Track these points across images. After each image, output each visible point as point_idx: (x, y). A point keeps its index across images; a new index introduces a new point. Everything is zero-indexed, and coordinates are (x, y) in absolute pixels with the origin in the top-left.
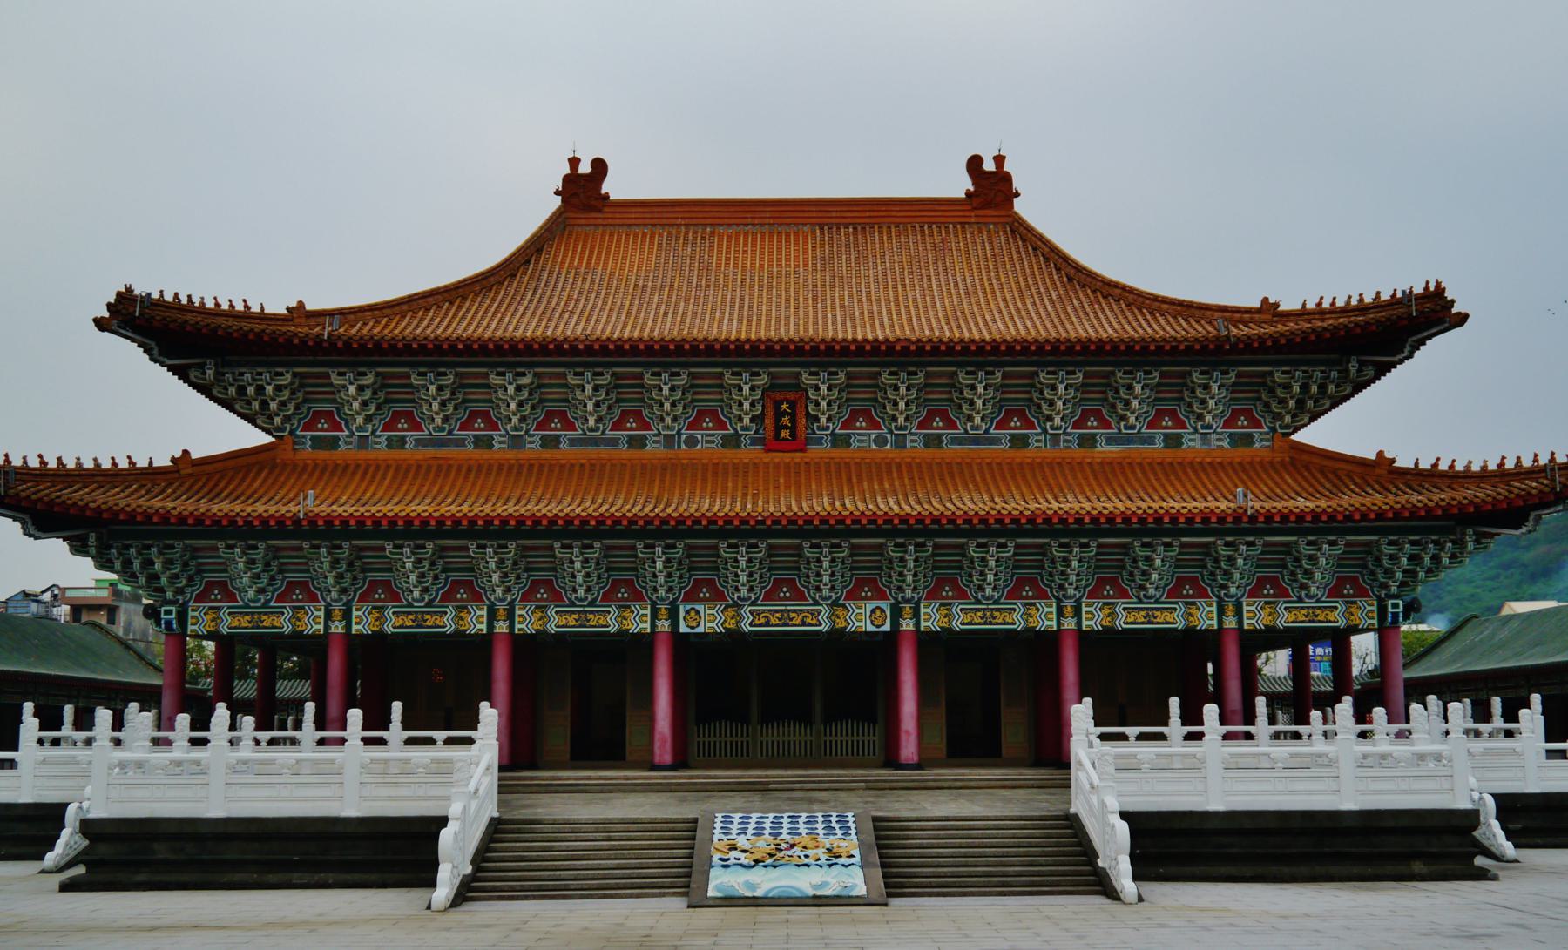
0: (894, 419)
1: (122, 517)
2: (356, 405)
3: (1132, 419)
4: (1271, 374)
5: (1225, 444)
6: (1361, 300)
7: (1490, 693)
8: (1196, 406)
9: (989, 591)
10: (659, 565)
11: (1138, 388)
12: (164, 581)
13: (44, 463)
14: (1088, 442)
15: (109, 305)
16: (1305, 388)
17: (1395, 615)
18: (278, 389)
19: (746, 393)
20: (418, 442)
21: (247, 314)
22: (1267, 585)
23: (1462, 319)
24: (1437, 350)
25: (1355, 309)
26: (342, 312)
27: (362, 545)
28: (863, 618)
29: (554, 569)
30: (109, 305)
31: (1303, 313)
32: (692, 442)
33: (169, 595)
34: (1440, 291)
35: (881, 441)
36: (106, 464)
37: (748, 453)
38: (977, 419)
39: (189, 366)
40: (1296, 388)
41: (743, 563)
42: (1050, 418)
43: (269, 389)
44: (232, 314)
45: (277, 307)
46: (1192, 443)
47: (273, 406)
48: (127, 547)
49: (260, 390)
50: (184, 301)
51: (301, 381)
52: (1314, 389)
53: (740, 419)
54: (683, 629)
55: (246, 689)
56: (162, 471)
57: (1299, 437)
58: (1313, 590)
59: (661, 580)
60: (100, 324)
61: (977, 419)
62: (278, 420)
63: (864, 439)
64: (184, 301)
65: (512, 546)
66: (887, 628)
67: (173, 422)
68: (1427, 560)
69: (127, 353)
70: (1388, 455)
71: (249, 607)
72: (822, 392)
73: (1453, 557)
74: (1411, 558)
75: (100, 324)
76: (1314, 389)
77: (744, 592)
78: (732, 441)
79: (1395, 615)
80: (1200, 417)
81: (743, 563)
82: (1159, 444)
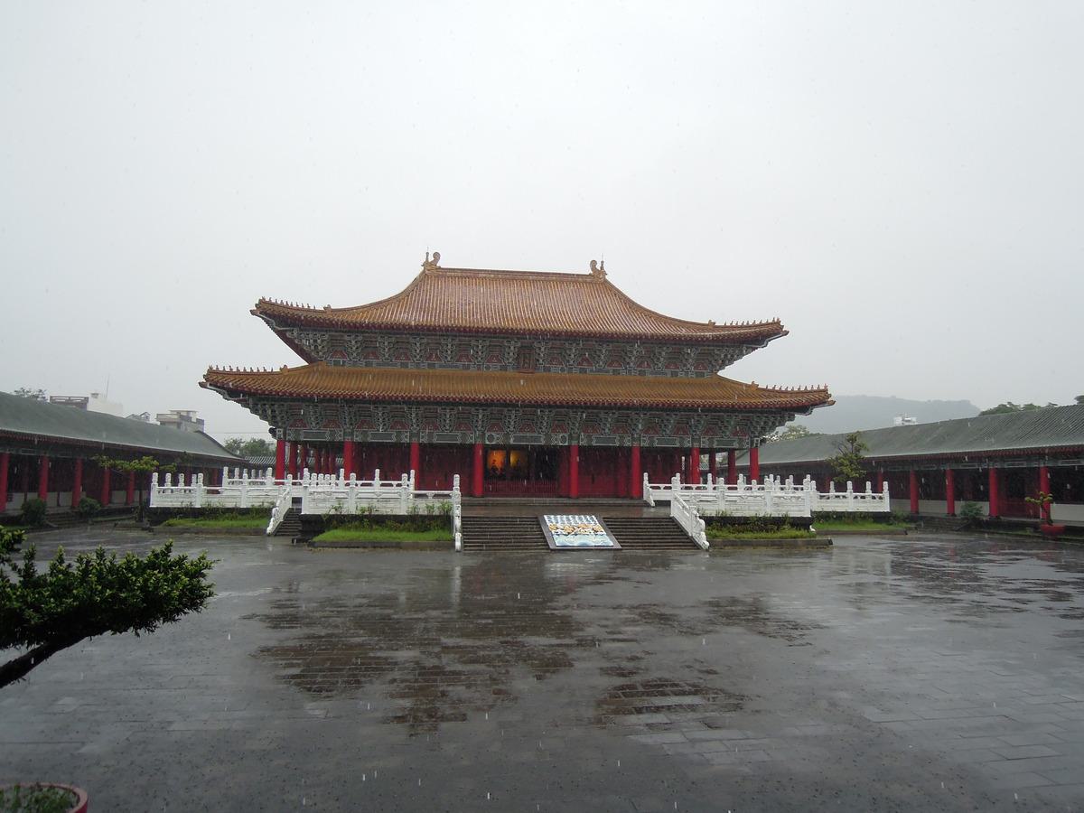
0: (568, 361)
1: (267, 392)
2: (354, 348)
3: (660, 365)
4: (713, 350)
5: (694, 376)
6: (748, 323)
7: (792, 472)
8: (684, 361)
9: (607, 430)
10: (480, 417)
11: (664, 353)
12: (279, 418)
13: (231, 369)
14: (642, 373)
15: (256, 305)
16: (726, 356)
17: (757, 444)
18: (322, 341)
19: (513, 347)
20: (378, 364)
21: (309, 310)
22: (708, 431)
23: (786, 333)
24: (774, 344)
25: (746, 327)
26: (344, 310)
27: (359, 406)
28: (558, 440)
29: (436, 418)
30: (256, 305)
31: (725, 327)
32: (488, 368)
33: (280, 424)
34: (778, 322)
35: (562, 370)
36: (255, 371)
37: (510, 373)
38: (601, 363)
39: (286, 331)
40: (722, 356)
41: (513, 417)
42: (628, 363)
43: (319, 341)
44: (303, 309)
45: (320, 307)
46: (681, 375)
47: (320, 348)
48: (265, 405)
49: (315, 341)
50: (285, 304)
51: (332, 339)
52: (729, 356)
53: (508, 359)
54: (488, 443)
55: (311, 461)
56: (277, 373)
57: (721, 373)
58: (728, 433)
59: (480, 423)
60: (253, 312)
61: (601, 363)
62: (320, 353)
63: (556, 370)
64: (285, 304)
65: (422, 408)
66: (566, 444)
67: (273, 355)
68: (770, 424)
69: (259, 323)
70: (756, 383)
71: (315, 431)
72: (543, 350)
73: (780, 422)
74: (765, 422)
75: (253, 312)
76: (729, 356)
77: (512, 428)
78: (504, 368)
79: (757, 444)
80: (685, 365)
81: (513, 417)
82: (669, 376)
